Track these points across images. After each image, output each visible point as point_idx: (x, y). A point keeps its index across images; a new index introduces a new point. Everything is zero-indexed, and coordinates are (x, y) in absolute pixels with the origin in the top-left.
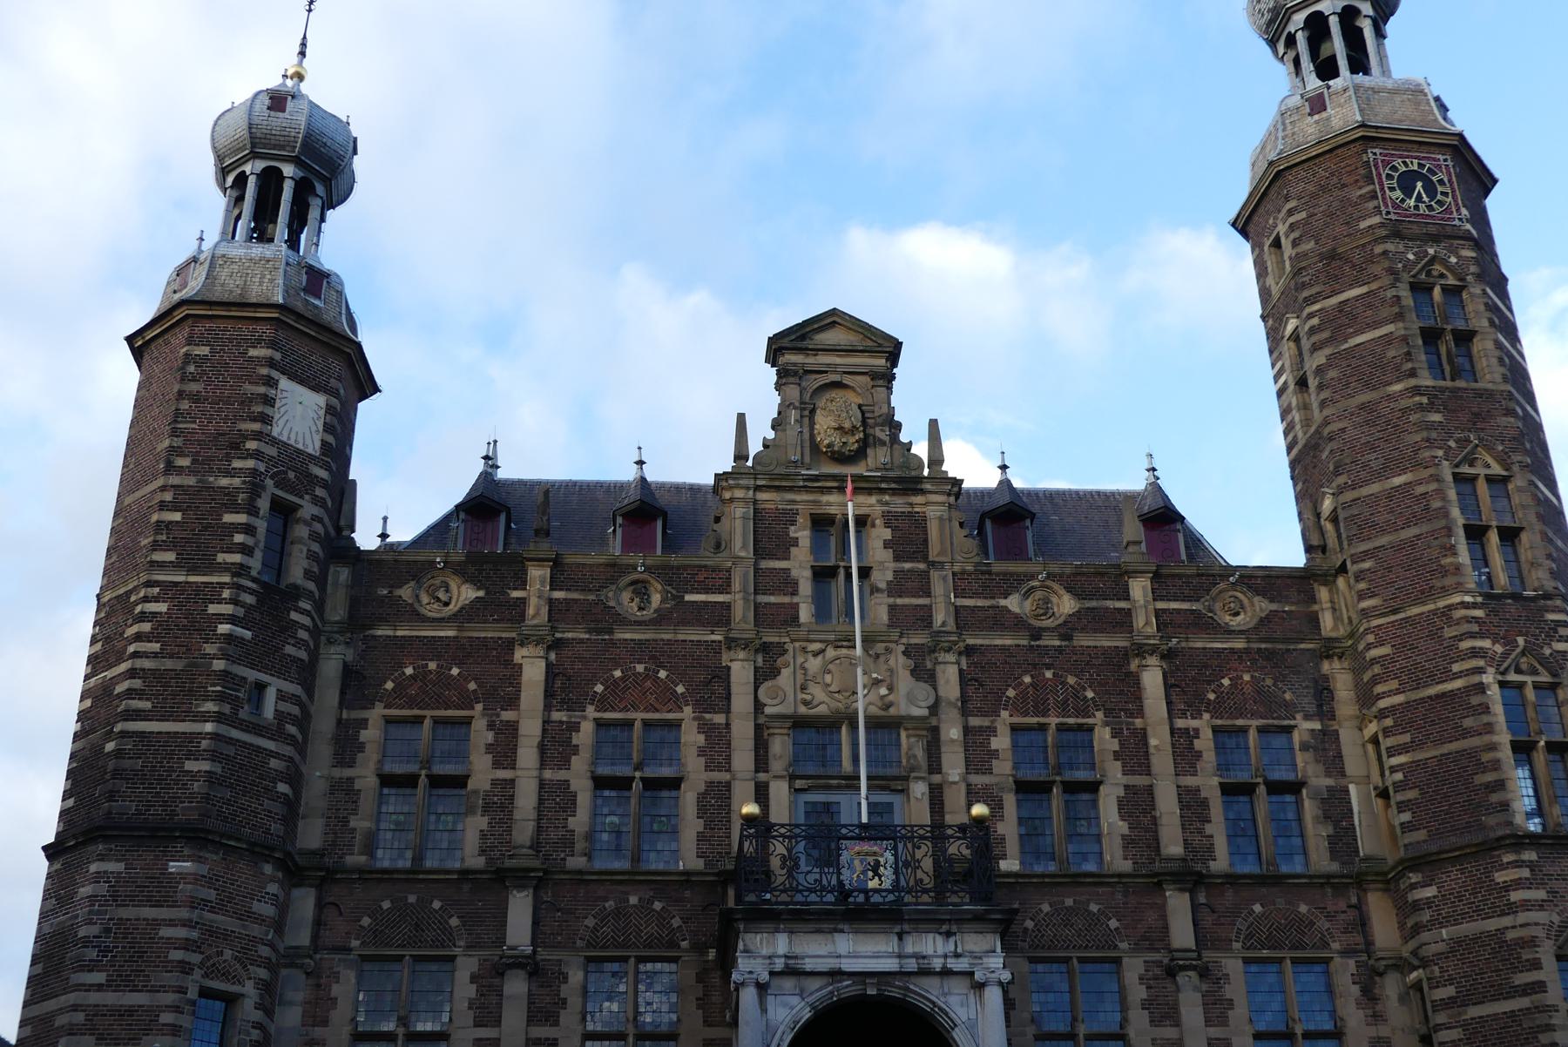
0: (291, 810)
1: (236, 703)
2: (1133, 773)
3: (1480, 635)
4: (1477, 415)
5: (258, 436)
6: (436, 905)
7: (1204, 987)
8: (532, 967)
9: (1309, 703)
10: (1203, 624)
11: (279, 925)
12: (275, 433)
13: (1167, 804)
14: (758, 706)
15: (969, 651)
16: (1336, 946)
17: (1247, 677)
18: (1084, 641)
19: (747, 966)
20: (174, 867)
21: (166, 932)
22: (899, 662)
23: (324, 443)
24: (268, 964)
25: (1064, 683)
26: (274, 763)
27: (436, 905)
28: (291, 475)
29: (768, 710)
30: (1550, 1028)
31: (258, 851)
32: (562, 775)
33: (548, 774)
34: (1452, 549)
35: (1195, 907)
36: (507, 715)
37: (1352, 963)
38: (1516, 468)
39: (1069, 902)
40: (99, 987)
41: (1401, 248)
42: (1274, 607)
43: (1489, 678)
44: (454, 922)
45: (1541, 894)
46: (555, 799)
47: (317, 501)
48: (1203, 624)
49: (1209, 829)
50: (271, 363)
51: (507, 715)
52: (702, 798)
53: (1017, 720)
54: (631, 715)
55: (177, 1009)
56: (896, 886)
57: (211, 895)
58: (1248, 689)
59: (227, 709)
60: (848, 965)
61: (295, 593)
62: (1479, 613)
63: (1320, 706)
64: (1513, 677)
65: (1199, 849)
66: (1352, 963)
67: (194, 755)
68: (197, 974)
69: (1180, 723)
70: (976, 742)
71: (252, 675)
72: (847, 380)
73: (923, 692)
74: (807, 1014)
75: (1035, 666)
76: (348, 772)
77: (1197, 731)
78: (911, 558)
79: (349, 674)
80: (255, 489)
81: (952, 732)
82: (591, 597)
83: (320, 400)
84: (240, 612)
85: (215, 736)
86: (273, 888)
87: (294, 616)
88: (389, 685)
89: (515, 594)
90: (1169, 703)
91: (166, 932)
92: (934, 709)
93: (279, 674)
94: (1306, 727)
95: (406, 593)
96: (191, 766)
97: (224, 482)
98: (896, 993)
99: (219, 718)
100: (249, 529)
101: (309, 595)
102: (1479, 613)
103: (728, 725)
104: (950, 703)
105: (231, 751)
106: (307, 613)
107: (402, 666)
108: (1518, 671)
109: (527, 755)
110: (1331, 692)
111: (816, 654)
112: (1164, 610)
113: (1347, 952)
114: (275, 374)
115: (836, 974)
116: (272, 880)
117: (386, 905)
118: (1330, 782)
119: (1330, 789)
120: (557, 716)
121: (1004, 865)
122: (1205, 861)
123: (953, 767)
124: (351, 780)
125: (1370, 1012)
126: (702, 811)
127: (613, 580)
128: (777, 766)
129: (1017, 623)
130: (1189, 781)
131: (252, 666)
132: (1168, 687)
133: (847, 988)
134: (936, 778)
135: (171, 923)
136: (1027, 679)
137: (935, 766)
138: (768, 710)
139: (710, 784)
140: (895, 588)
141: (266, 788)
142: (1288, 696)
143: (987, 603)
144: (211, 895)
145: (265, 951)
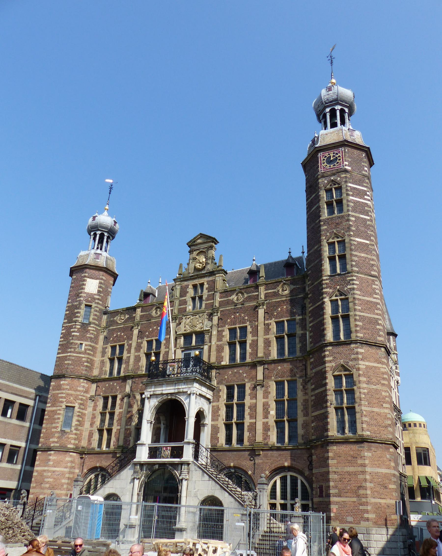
0: (90, 368)
1: (75, 348)
2: (254, 336)
3: (327, 288)
4: (337, 224)
5: (81, 293)
6: (115, 384)
7: (263, 389)
8: (128, 396)
9: (299, 312)
10: (276, 294)
11: (87, 392)
12: (86, 291)
13: (261, 344)
14: (176, 332)
15: (221, 311)
16: (298, 376)
17: (285, 307)
18: (247, 305)
19: (147, 394)
20: (62, 382)
21: (59, 395)
22: (206, 316)
23: (98, 290)
24: (81, 400)
25: (241, 316)
26: (83, 359)
27: (115, 384)
28: (90, 299)
29: (178, 333)
30: (326, 395)
31: (79, 377)
32: (139, 354)
33: (136, 354)
34: (321, 265)
35: (264, 369)
36: (130, 342)
37: (301, 380)
38: (346, 237)
39: (235, 371)
40: (50, 407)
41: (324, 180)
42: (295, 287)
43: (327, 300)
44: (118, 387)
45: (331, 358)
46: (138, 359)
47: (96, 303)
48: (276, 294)
49: (270, 348)
50: (85, 276)
51: (130, 342)
52: (164, 355)
53: (230, 327)
54: (152, 338)
55: (59, 410)
56: (177, 373)
57: (68, 387)
58: (285, 310)
59: (73, 350)
60: (164, 392)
61: (90, 323)
62: (328, 281)
63: (302, 312)
64: (334, 298)
65: (267, 353)
66: (301, 380)
67: (66, 360)
68: (65, 403)
69: (266, 322)
70: (220, 333)
71: (79, 342)
72: (202, 250)
73: (210, 324)
74: (157, 403)
75: (235, 313)
76: (103, 358)
77: (270, 323)
78: (211, 291)
79: (106, 338)
80: (80, 304)
81: (215, 332)
82: (148, 313)
83: (98, 281)
84: (76, 330)
85: (69, 356)
86: (82, 384)
87: (89, 328)
88: (111, 339)
89: (134, 315)
90: (264, 317)
91: (59, 395)
92: (211, 327)
93: (86, 341)
94: (298, 318)
95: (115, 319)
96: (66, 362)
97: (76, 303)
98: (174, 398)
99: (70, 352)
100: (78, 313)
101: (94, 323)
102: (328, 281)
103: (170, 338)
104: (215, 326)
105: (74, 358)
106: (93, 327)
107: (114, 334)
108: (336, 296)
109: (133, 350)
110: (306, 307)
111: (188, 318)
112: (267, 293)
113: (300, 377)
114: (85, 278)
115: (162, 394)
116: (83, 383)
117: (107, 385)
118: (302, 332)
119: (302, 334)
120: (139, 341)
121: (223, 363)
122: (268, 357)
123: (213, 342)
124: (104, 360)
125: (304, 392)
126: (163, 357)
127: (152, 309)
128: (178, 346)
129: (232, 302)
130: (267, 337)
131: (79, 340)
132: (265, 313)
133: (165, 397)
134: (210, 344)
135: (60, 393)
136: (233, 316)
137: (210, 342)
138: (178, 333)
139: (165, 352)
140: (207, 299)
141: (82, 365)
142: (294, 311)
143: (226, 299)
144: (68, 387)
145: (80, 397)
